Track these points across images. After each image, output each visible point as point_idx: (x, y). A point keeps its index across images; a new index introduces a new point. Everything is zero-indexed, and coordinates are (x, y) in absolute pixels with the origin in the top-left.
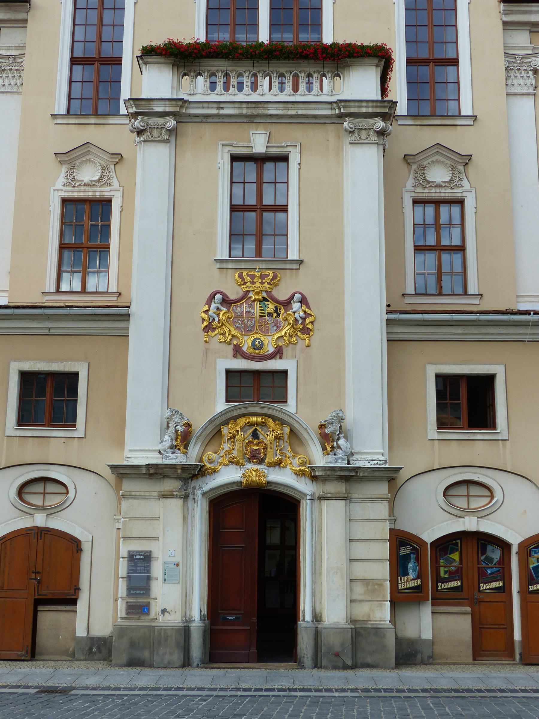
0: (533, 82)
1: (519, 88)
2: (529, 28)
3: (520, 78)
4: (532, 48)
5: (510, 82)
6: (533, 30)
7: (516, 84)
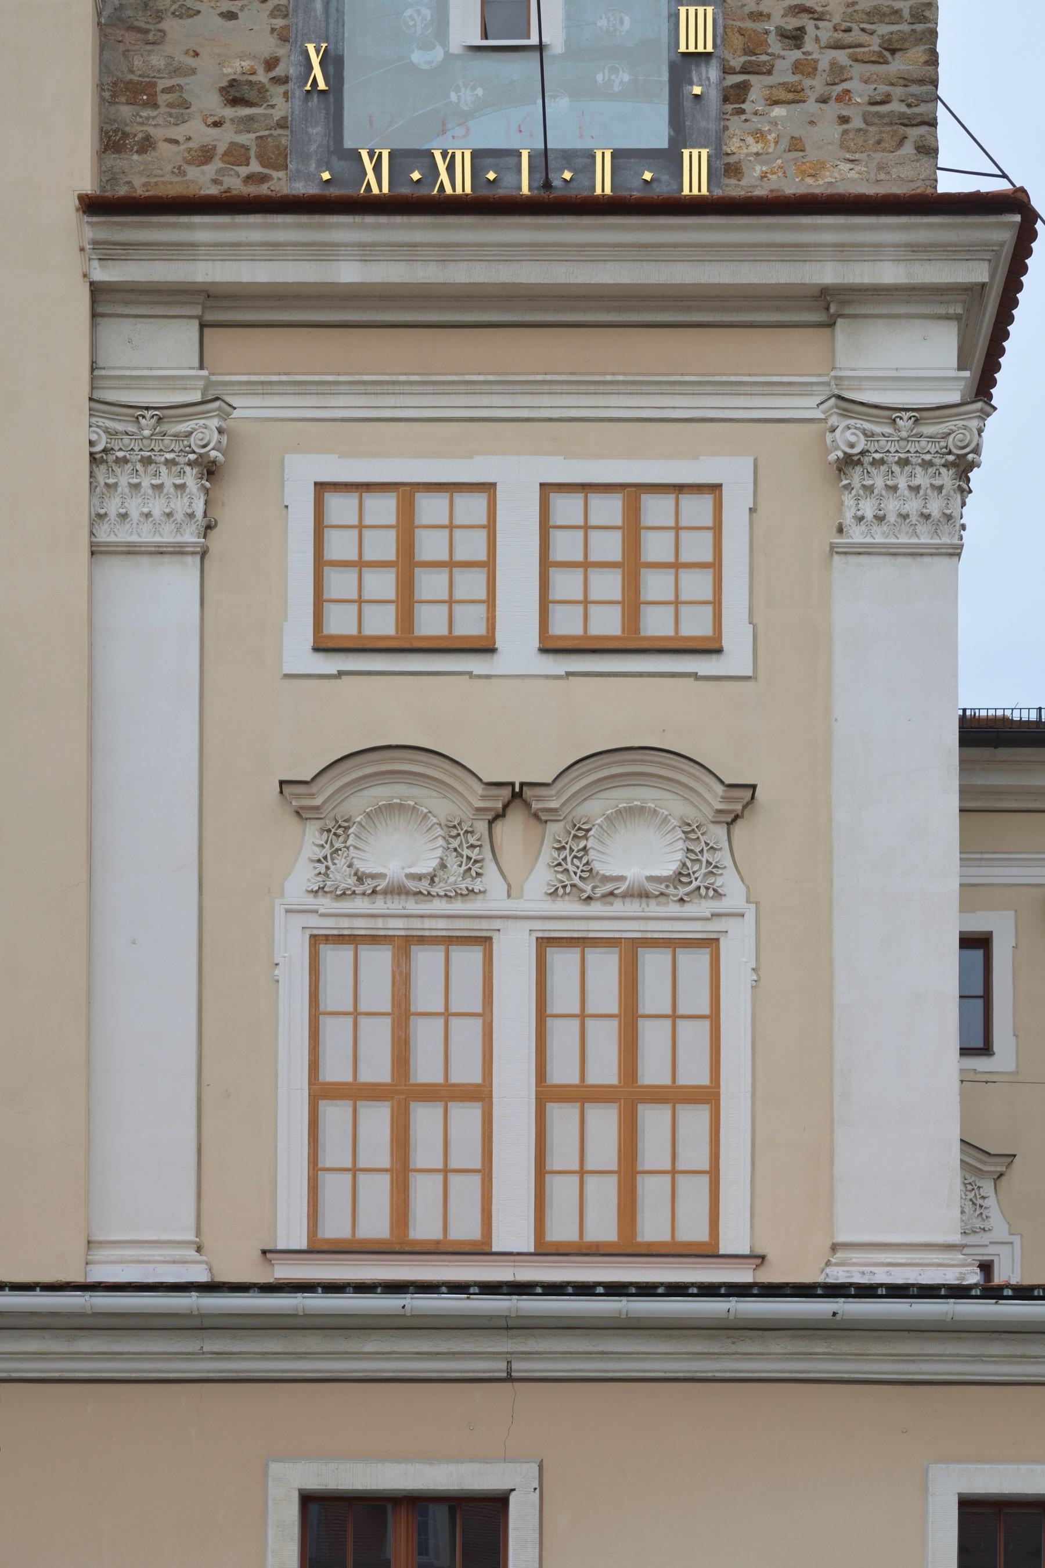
0: (199, 507)
1: (147, 526)
2: (197, 311)
3: (150, 491)
4: (201, 384)
5: (113, 507)
6: (210, 317)
7: (135, 514)
